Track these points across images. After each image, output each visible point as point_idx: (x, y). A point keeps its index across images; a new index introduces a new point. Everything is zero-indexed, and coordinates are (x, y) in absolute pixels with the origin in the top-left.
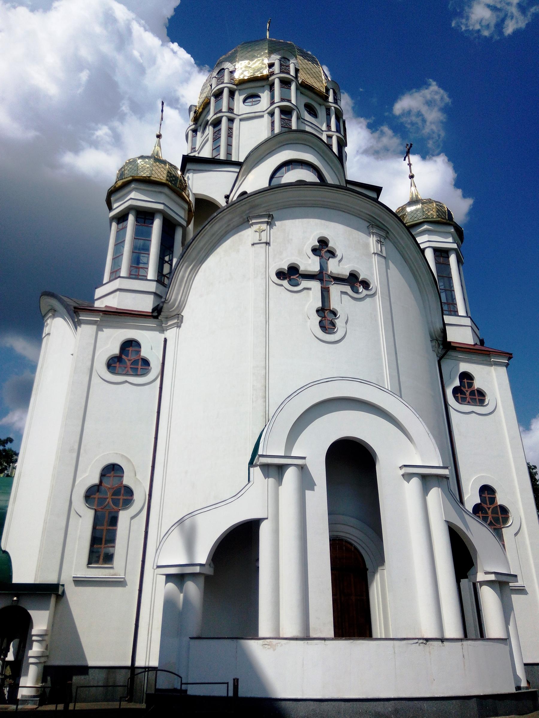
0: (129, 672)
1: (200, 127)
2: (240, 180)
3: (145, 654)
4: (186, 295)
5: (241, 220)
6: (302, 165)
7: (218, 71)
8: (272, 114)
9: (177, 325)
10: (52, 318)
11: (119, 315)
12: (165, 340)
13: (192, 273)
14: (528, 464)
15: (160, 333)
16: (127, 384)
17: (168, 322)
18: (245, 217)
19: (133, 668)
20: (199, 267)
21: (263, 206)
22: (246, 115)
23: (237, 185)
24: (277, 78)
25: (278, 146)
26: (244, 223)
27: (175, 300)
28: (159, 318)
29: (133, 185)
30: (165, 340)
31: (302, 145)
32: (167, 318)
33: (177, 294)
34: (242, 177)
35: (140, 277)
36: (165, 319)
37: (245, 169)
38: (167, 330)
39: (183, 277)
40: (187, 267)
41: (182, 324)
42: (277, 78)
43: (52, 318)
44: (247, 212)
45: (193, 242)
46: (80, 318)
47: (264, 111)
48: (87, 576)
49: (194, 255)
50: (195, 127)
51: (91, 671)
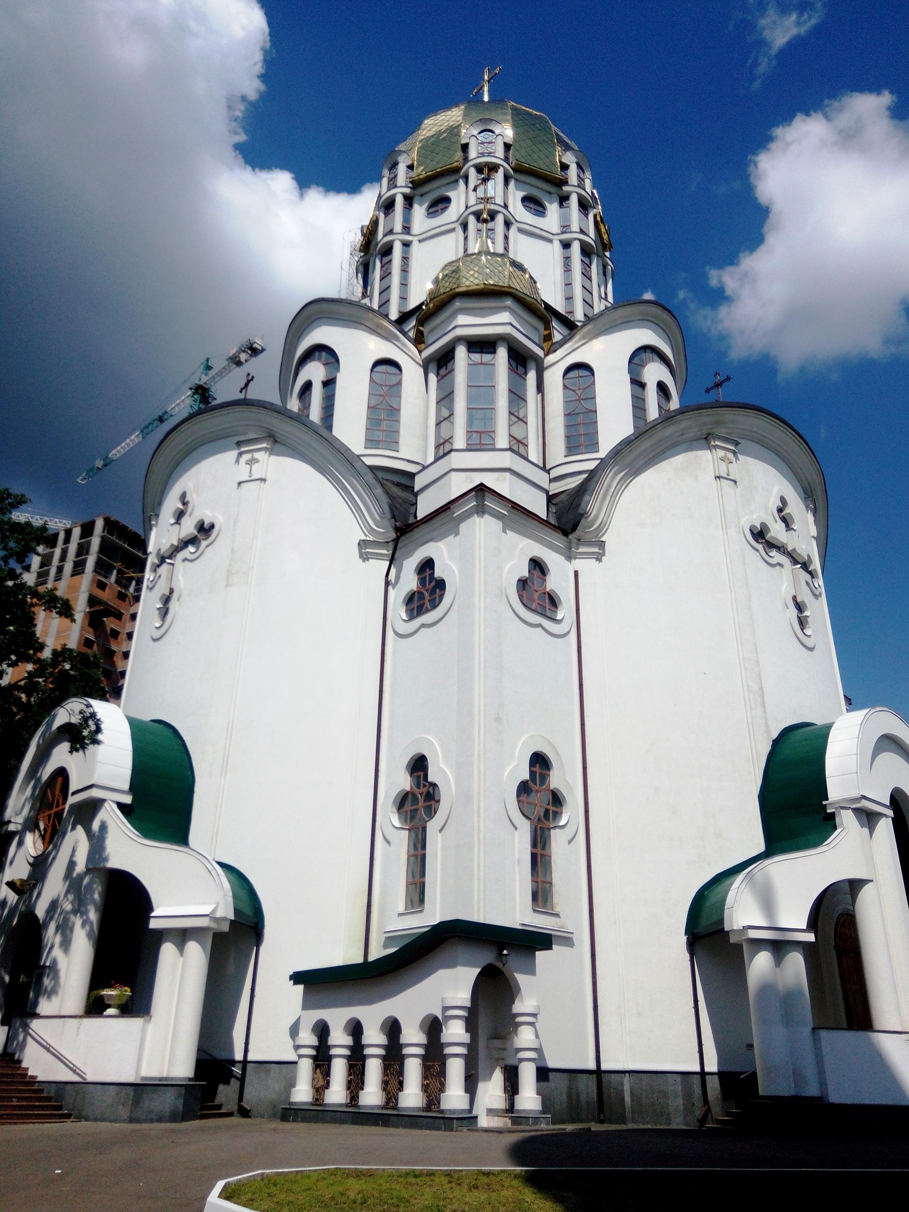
0: (698, 1077)
1: (419, 197)
2: (576, 342)
3: (70, 1060)
4: (610, 513)
5: (699, 433)
6: (645, 352)
7: (482, 129)
8: (566, 245)
9: (598, 556)
10: (268, 453)
11: (528, 515)
12: (576, 574)
13: (621, 483)
14: (871, 833)
15: (566, 559)
16: (540, 628)
17: (581, 547)
18: (705, 432)
19: (598, 1073)
20: (631, 479)
21: (729, 426)
22: (529, 226)
23: (569, 348)
24: (577, 193)
25: (637, 318)
26: (700, 439)
27: (596, 517)
28: (570, 537)
29: (510, 302)
30: (576, 574)
31: (651, 323)
32: (579, 540)
33: (600, 509)
34: (580, 340)
35: (483, 447)
36: (576, 541)
37: (588, 330)
38: (575, 558)
39: (609, 487)
40: (616, 474)
41: (603, 558)
42: (577, 193)
43: (268, 453)
44: (710, 426)
45: (635, 441)
46: (486, 503)
47: (553, 234)
48: (537, 925)
49: (629, 459)
50: (410, 193)
51: (552, 1075)
